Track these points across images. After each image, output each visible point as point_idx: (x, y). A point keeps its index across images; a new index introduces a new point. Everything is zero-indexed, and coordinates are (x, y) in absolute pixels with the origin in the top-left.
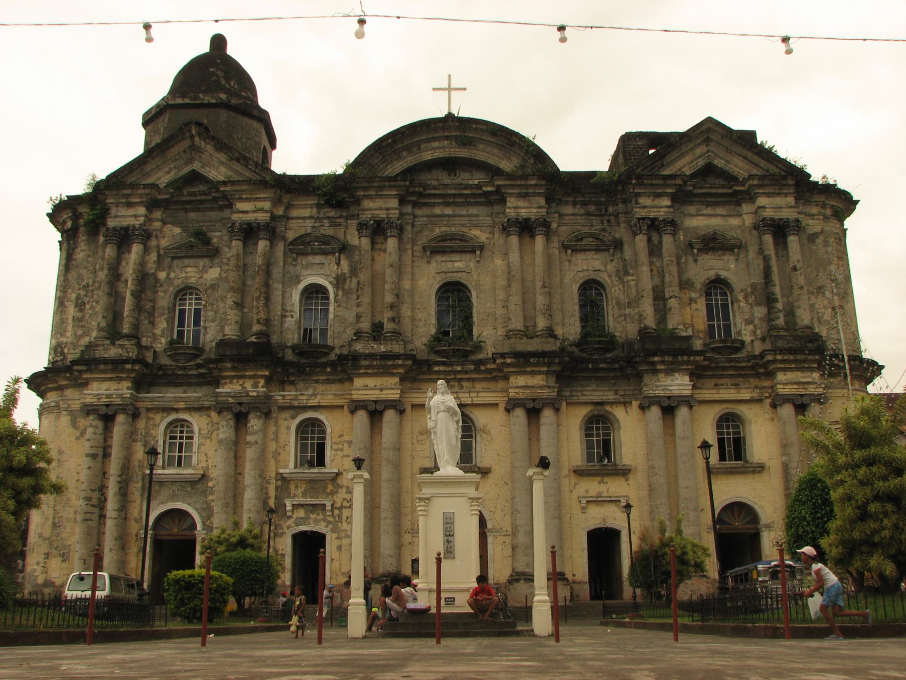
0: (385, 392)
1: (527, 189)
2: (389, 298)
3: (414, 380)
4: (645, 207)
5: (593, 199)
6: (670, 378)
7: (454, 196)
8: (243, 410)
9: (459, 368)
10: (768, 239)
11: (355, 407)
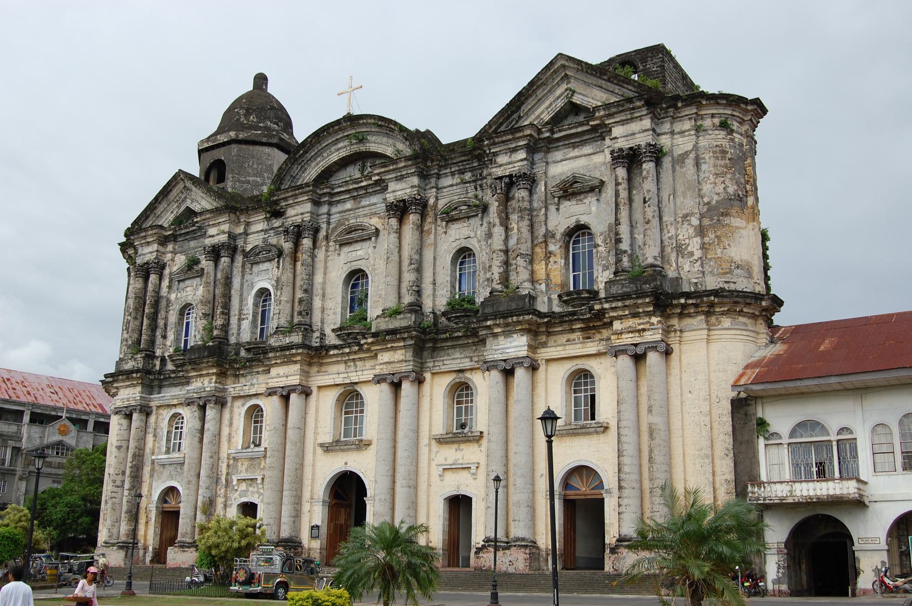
0: (290, 378)
1: (400, 172)
3: (321, 364)
4: (500, 166)
5: (467, 166)
6: (509, 340)
9: (347, 350)
10: (621, 172)
11: (271, 393)
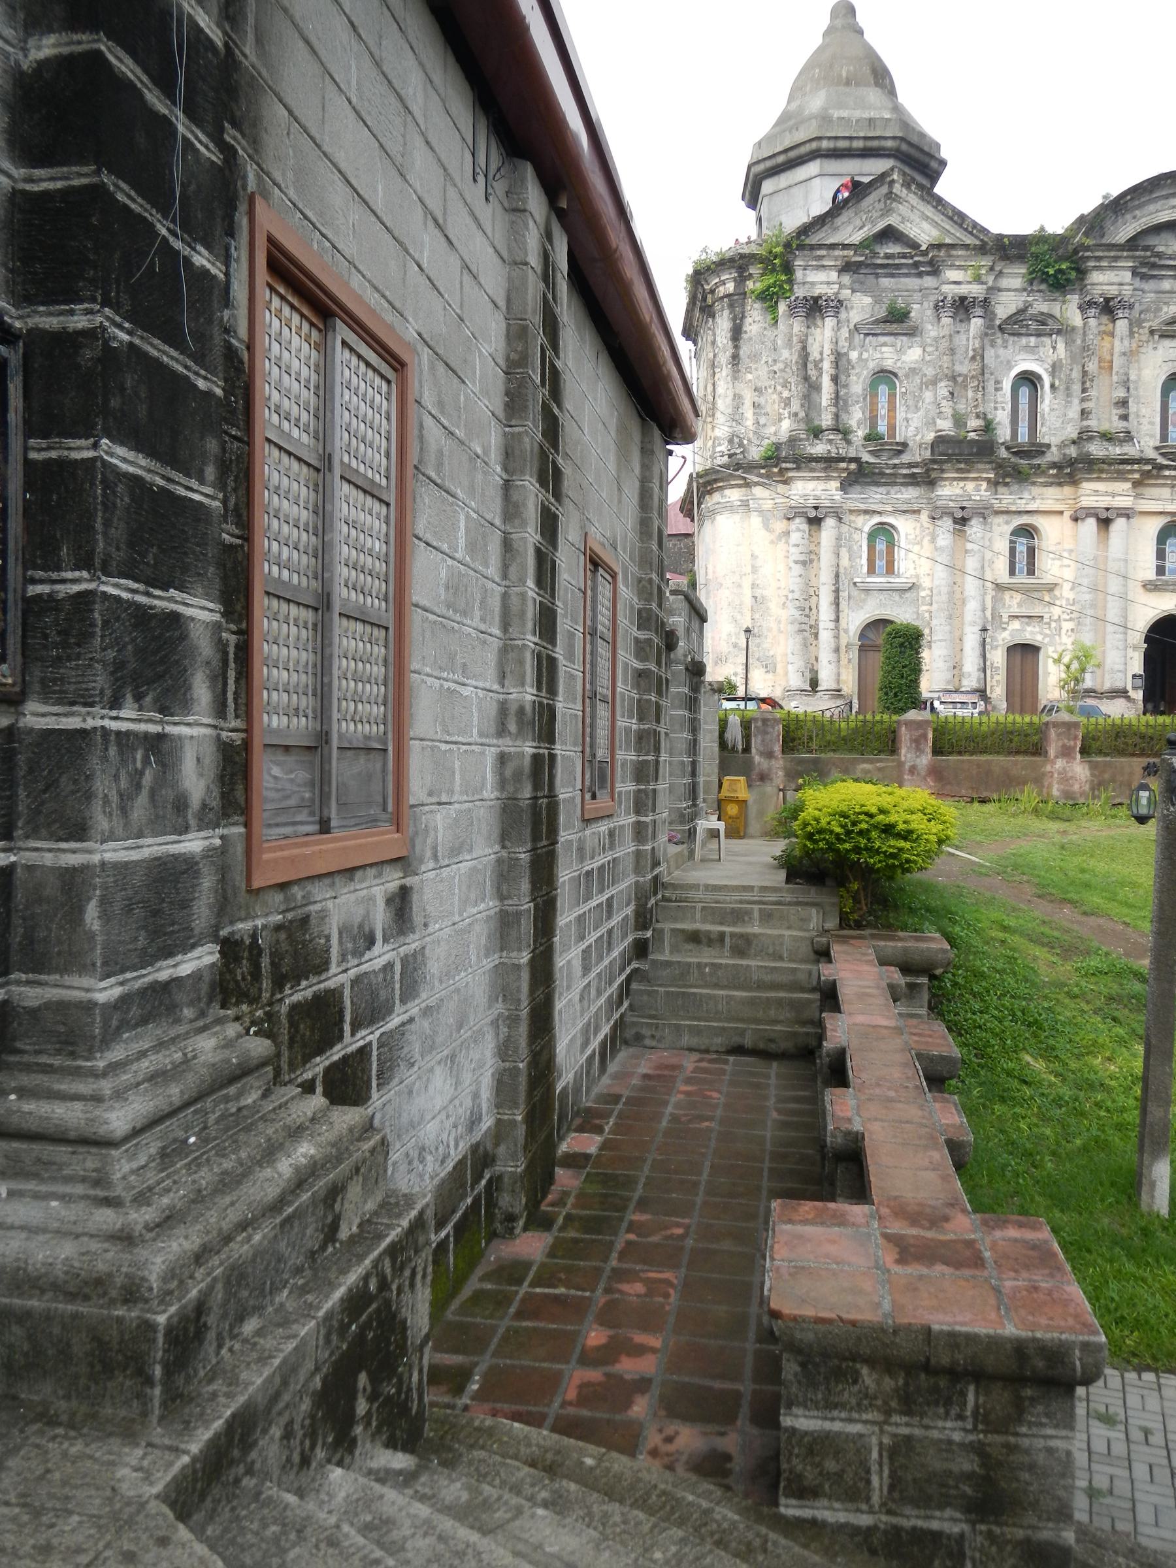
2: (1121, 393)
8: (965, 514)
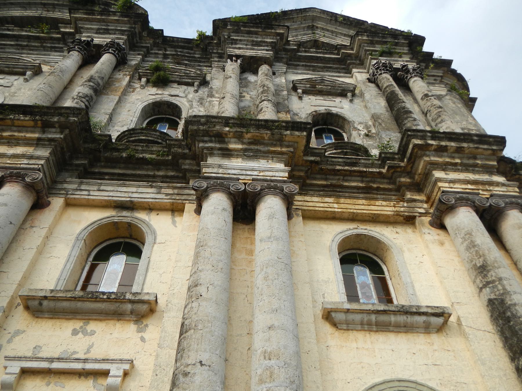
7: (29, 38)
